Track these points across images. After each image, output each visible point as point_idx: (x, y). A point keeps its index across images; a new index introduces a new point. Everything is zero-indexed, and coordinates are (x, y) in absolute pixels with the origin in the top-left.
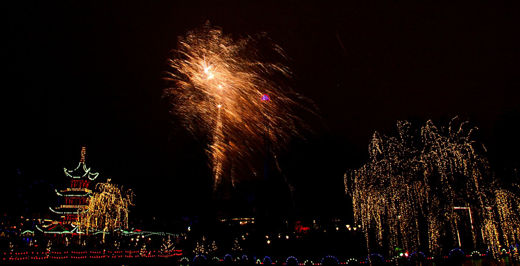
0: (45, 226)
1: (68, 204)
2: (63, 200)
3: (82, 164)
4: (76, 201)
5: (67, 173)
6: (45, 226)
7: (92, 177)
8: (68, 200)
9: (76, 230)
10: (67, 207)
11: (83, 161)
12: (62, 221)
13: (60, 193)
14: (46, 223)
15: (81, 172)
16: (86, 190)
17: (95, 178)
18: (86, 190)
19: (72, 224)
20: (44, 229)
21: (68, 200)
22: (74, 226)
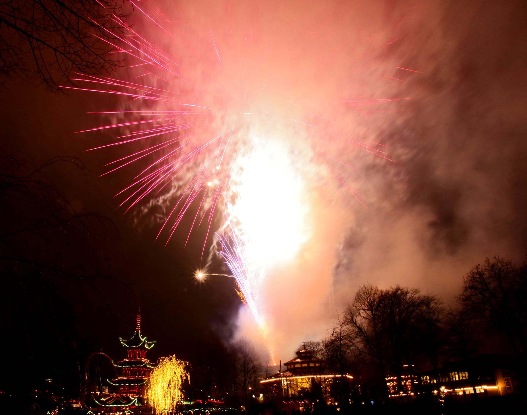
0: (104, 399)
1: (125, 376)
2: (120, 372)
4: (134, 373)
5: (122, 343)
6: (104, 399)
7: (149, 345)
9: (135, 402)
10: (126, 378)
12: (121, 393)
13: (117, 364)
14: (105, 396)
17: (152, 346)
21: (126, 371)
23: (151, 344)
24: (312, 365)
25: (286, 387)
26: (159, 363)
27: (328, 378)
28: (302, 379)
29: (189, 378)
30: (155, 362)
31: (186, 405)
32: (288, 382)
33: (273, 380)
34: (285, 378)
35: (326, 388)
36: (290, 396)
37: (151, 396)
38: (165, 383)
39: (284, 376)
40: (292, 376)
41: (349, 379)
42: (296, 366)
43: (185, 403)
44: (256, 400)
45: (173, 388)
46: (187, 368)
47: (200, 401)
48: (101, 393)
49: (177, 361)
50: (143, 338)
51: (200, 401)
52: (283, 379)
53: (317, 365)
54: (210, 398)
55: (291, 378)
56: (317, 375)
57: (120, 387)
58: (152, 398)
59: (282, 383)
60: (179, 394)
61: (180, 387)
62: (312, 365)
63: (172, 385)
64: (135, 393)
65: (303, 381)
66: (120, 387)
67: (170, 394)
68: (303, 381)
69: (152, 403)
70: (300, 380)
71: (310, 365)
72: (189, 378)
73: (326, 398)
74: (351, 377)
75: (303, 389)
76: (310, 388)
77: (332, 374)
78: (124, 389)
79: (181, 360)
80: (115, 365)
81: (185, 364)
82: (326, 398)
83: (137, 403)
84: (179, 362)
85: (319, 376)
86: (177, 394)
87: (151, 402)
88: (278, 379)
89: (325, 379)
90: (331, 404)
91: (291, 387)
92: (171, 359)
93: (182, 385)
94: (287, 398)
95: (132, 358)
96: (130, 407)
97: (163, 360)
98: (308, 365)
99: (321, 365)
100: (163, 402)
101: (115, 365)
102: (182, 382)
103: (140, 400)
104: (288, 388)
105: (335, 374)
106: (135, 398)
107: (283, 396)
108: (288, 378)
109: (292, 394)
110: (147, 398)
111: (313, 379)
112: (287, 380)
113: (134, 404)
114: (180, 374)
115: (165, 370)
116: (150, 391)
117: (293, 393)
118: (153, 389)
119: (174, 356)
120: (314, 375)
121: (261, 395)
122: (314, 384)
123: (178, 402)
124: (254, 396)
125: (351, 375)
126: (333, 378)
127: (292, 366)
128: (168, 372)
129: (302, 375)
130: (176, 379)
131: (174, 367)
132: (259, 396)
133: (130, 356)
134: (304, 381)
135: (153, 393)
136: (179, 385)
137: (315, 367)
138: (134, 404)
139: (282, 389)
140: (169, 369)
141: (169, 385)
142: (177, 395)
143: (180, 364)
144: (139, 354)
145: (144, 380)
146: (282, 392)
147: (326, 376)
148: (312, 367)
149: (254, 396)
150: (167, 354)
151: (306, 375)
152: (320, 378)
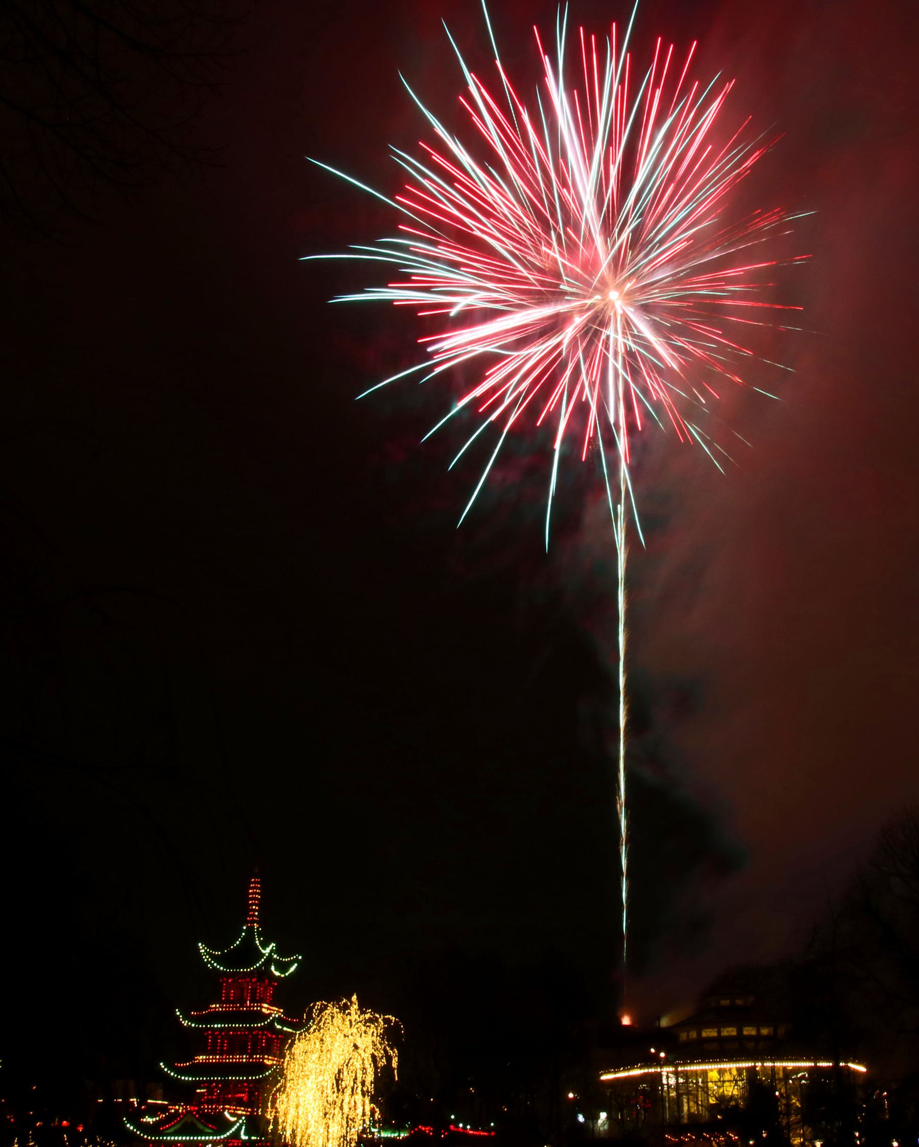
3: (250, 930)
4: (237, 1044)
5: (206, 958)
7: (283, 967)
8: (215, 1039)
9: (239, 1129)
11: (253, 922)
12: (199, 1104)
14: (153, 1110)
15: (249, 953)
16: (265, 1009)
17: (292, 969)
18: (265, 1009)
19: (226, 1113)
20: (146, 1128)
21: (215, 1039)
22: (233, 1119)
23: (290, 964)
24: (749, 1031)
25: (673, 1094)
26: (310, 1017)
27: (796, 1070)
28: (721, 1072)
29: (395, 1064)
30: (300, 1017)
31: (387, 1139)
32: (681, 1080)
33: (636, 1072)
34: (671, 1069)
35: (788, 1098)
36: (685, 1121)
37: (285, 1114)
38: (327, 1077)
39: (667, 1062)
40: (692, 1063)
41: (855, 1072)
42: (704, 1034)
43: (384, 1134)
44: (586, 1130)
45: (348, 1091)
46: (390, 1035)
47: (427, 1129)
48: (142, 1102)
49: (363, 1013)
50: (265, 946)
51: (427, 1129)
52: (666, 1070)
53: (765, 1032)
54: (456, 1122)
55: (688, 1068)
56: (763, 1060)
57: (199, 1085)
58: (290, 1118)
59: (665, 1082)
60: (368, 1108)
61: (369, 1086)
62: (749, 1031)
63: (347, 1081)
64: (240, 1103)
65: (723, 1078)
66: (199, 1085)
67: (341, 1108)
68: (723, 1078)
69: (288, 1133)
70: (714, 1076)
71: (745, 1033)
72: (395, 1064)
73: (788, 1126)
74: (862, 1069)
75: (722, 1099)
76: (742, 1097)
77: (808, 1059)
78: (210, 1091)
79: (375, 1010)
80: (185, 1023)
81: (386, 1021)
82: (788, 1126)
83: (245, 1134)
84: (367, 1016)
85: (768, 1064)
86: (361, 1107)
87: (284, 1129)
88: (652, 1070)
89: (787, 1073)
90: (802, 1144)
91: (688, 1093)
92: (344, 1009)
93: (377, 1081)
94: (678, 1127)
95: (234, 1002)
96: (225, 1142)
97: (323, 1009)
98: (740, 1031)
99: (775, 1031)
100: (322, 1129)
101: (185, 1023)
102: (376, 1073)
103: (255, 1124)
104: (679, 1096)
105: (815, 1060)
106: (239, 1117)
107: (664, 1120)
108: (680, 1069)
109: (690, 1115)
110: (276, 1119)
111: (752, 1071)
112: (677, 1074)
113: (237, 1134)
114: (370, 1050)
115: (328, 1040)
116: (284, 1096)
117: (692, 1110)
118: (293, 1094)
119: (354, 998)
120: (755, 1060)
121: (603, 1115)
122: (757, 1087)
123: (364, 1130)
124: (581, 1118)
125: (859, 1063)
126: (809, 1070)
127: (694, 1035)
128: (337, 1044)
129: (721, 1061)
130: (358, 1065)
131: (354, 1030)
132: (598, 1117)
133: (227, 996)
134: (727, 1077)
135: (293, 1104)
136: (368, 1083)
137: (758, 1038)
138: (237, 1134)
139: (662, 1098)
140: (340, 1036)
141: (338, 1080)
142: (360, 1111)
143: (372, 1021)
144: (254, 991)
145: (268, 1067)
146: (664, 1107)
147: (790, 1065)
148: (750, 1038)
149: (581, 1118)
150: (335, 994)
151: (731, 1059)
152: (773, 1068)
